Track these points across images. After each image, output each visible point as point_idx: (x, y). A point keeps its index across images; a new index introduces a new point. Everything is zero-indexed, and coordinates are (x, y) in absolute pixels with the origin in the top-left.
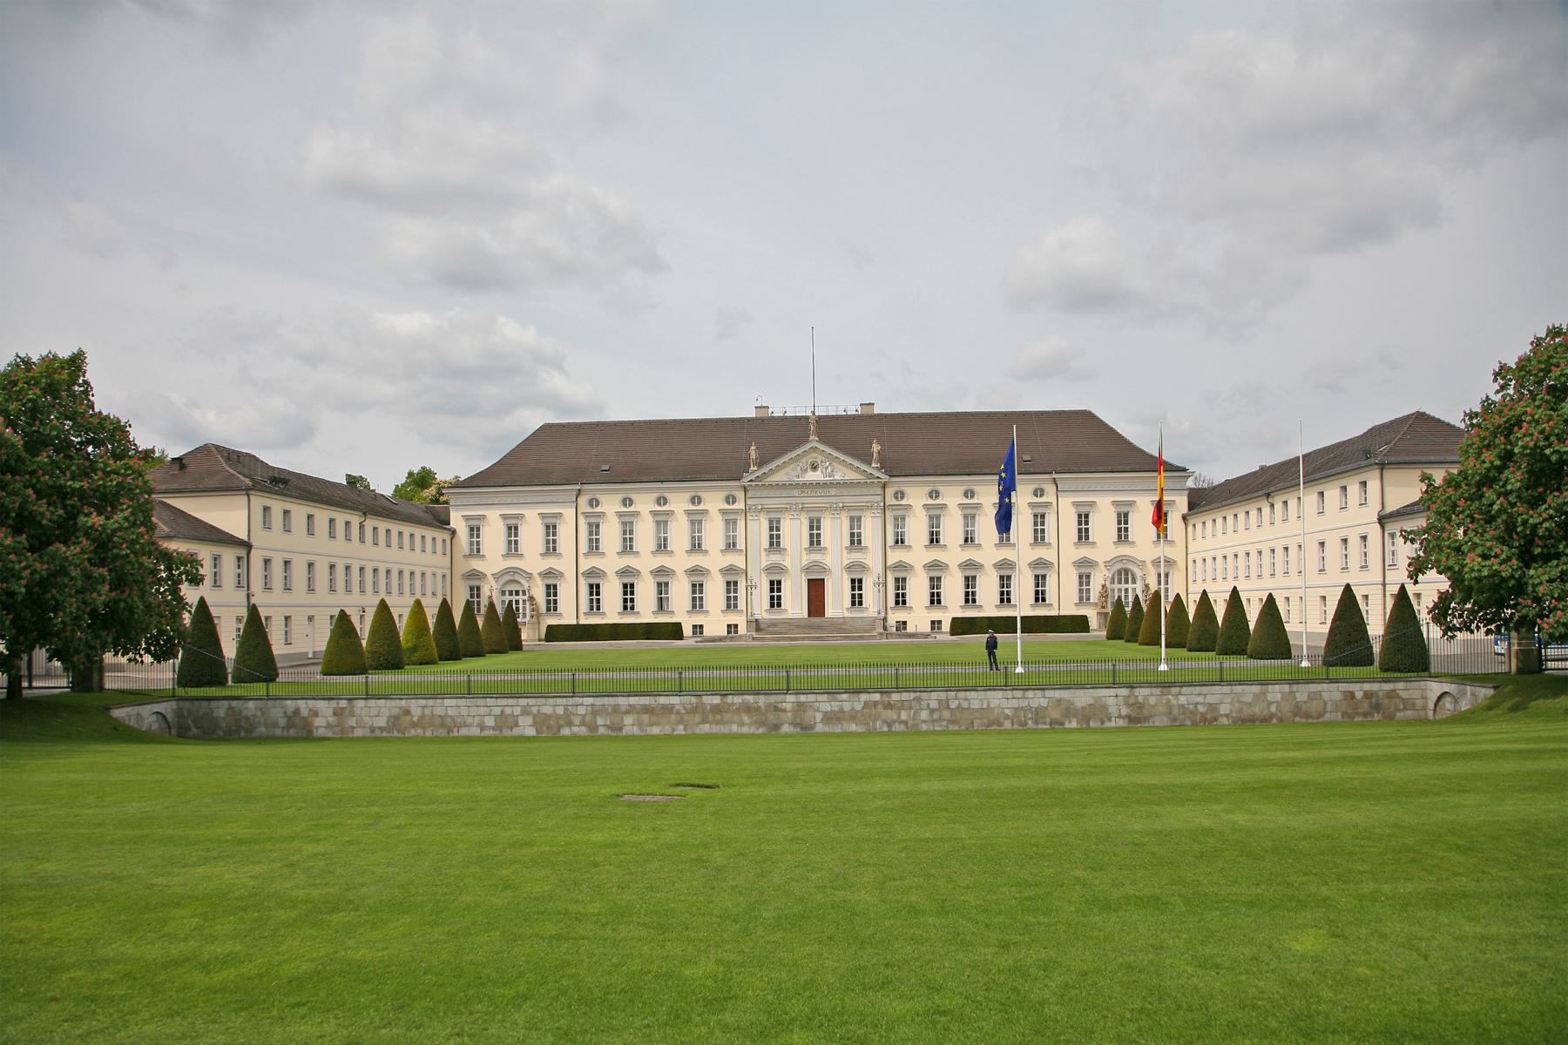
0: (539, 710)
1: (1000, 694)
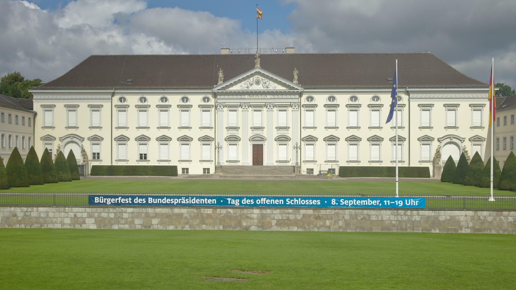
0: (99, 216)
1: (389, 212)
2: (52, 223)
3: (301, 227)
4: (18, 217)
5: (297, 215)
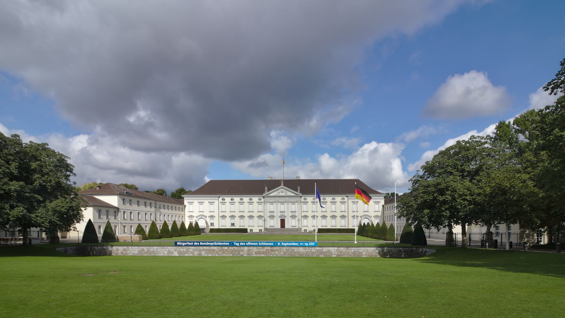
1: (302, 248)
2: (160, 253)
3: (265, 255)
4: (145, 251)
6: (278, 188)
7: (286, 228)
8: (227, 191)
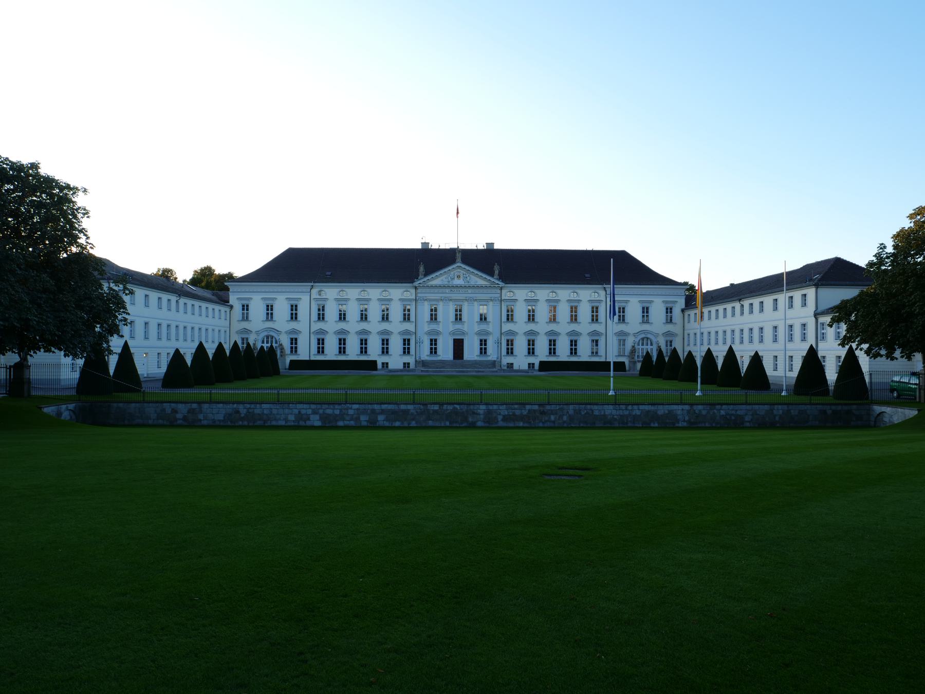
0: (323, 412)
1: (611, 407)
5: (523, 411)
6: (450, 268)
7: (464, 359)
8: (329, 273)
